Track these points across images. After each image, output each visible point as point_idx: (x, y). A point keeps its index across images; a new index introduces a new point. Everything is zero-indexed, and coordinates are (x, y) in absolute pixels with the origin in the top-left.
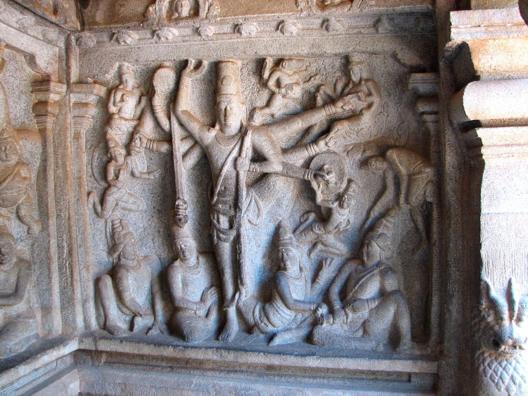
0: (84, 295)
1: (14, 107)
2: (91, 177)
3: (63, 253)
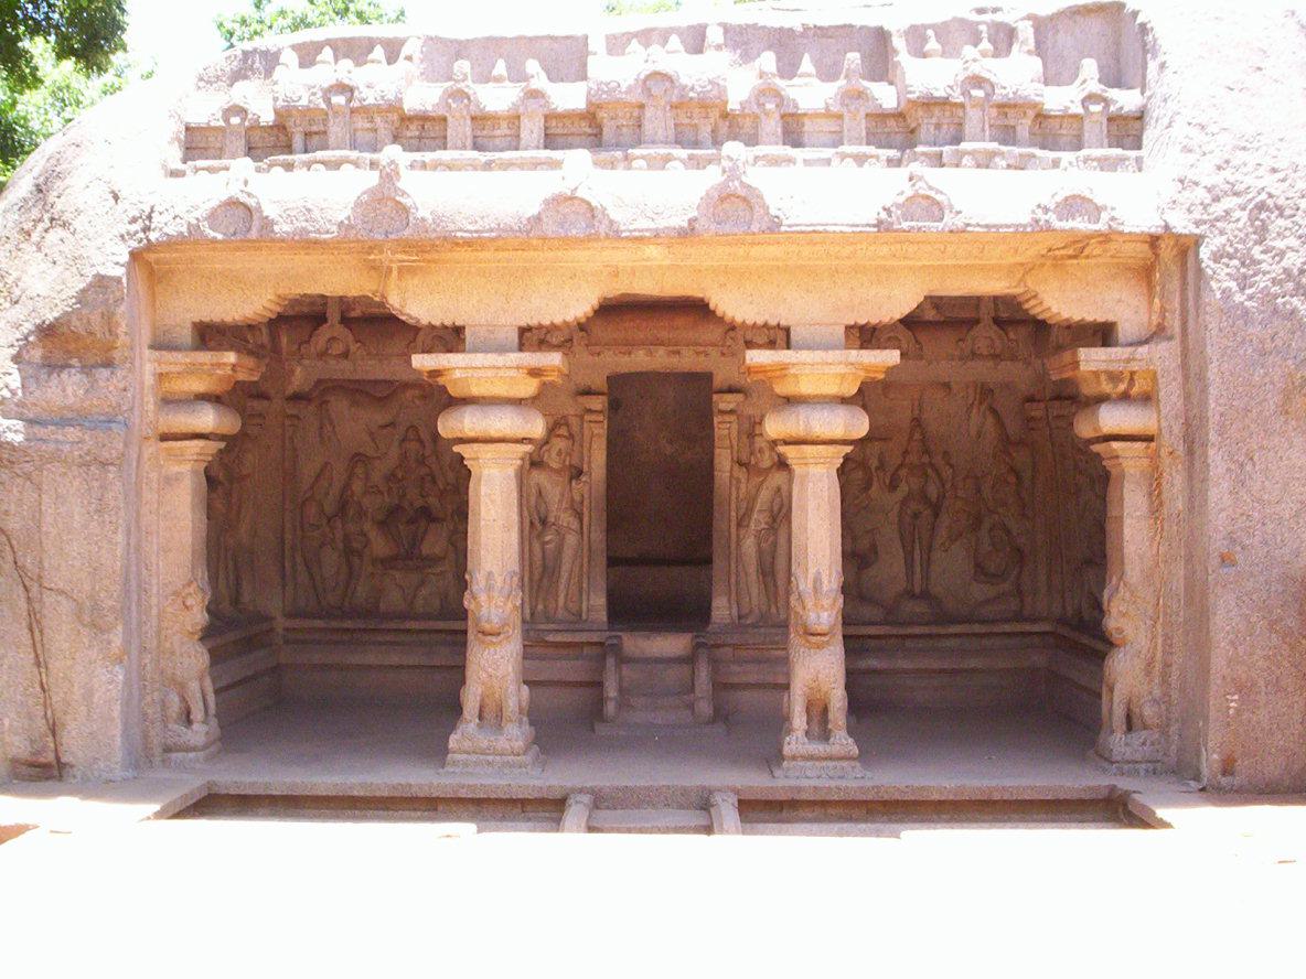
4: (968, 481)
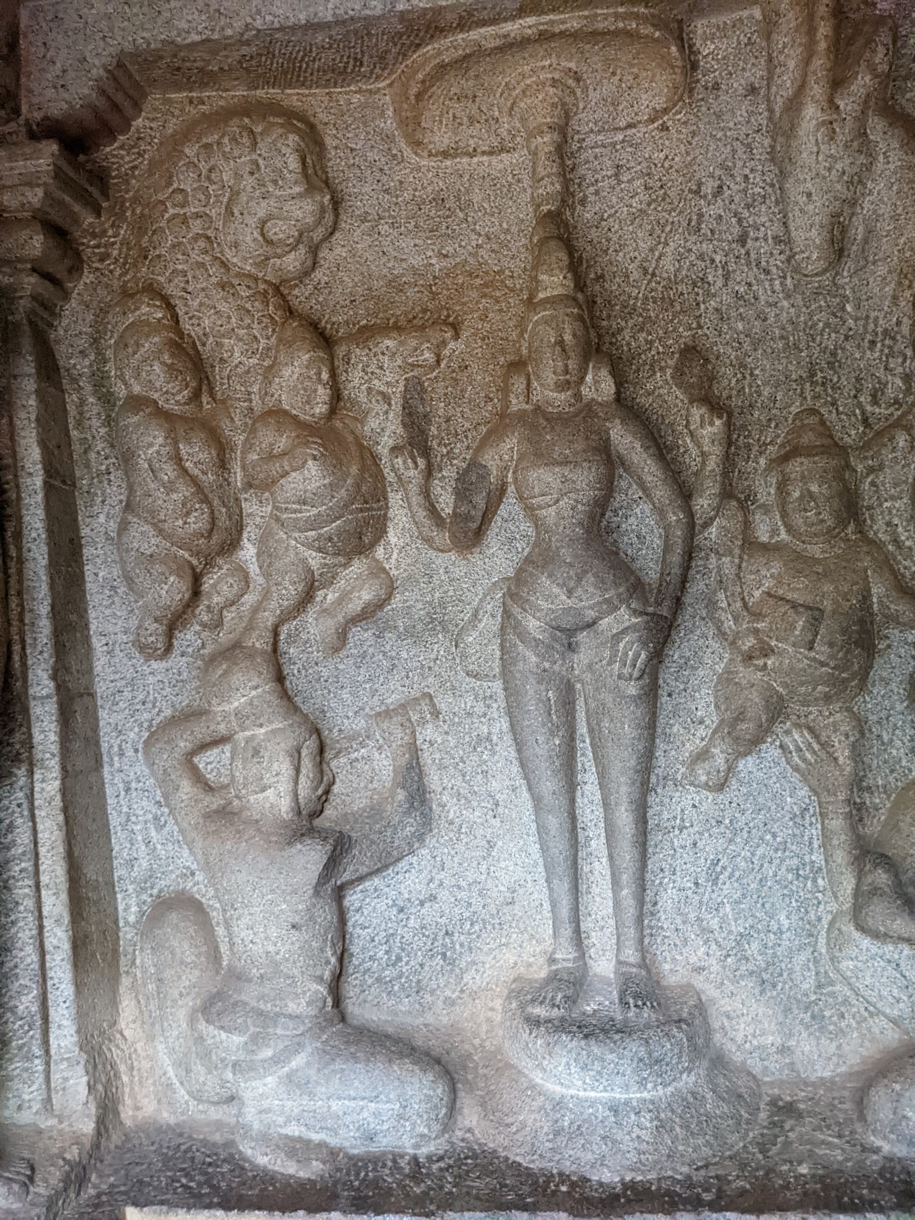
4: (796, 467)
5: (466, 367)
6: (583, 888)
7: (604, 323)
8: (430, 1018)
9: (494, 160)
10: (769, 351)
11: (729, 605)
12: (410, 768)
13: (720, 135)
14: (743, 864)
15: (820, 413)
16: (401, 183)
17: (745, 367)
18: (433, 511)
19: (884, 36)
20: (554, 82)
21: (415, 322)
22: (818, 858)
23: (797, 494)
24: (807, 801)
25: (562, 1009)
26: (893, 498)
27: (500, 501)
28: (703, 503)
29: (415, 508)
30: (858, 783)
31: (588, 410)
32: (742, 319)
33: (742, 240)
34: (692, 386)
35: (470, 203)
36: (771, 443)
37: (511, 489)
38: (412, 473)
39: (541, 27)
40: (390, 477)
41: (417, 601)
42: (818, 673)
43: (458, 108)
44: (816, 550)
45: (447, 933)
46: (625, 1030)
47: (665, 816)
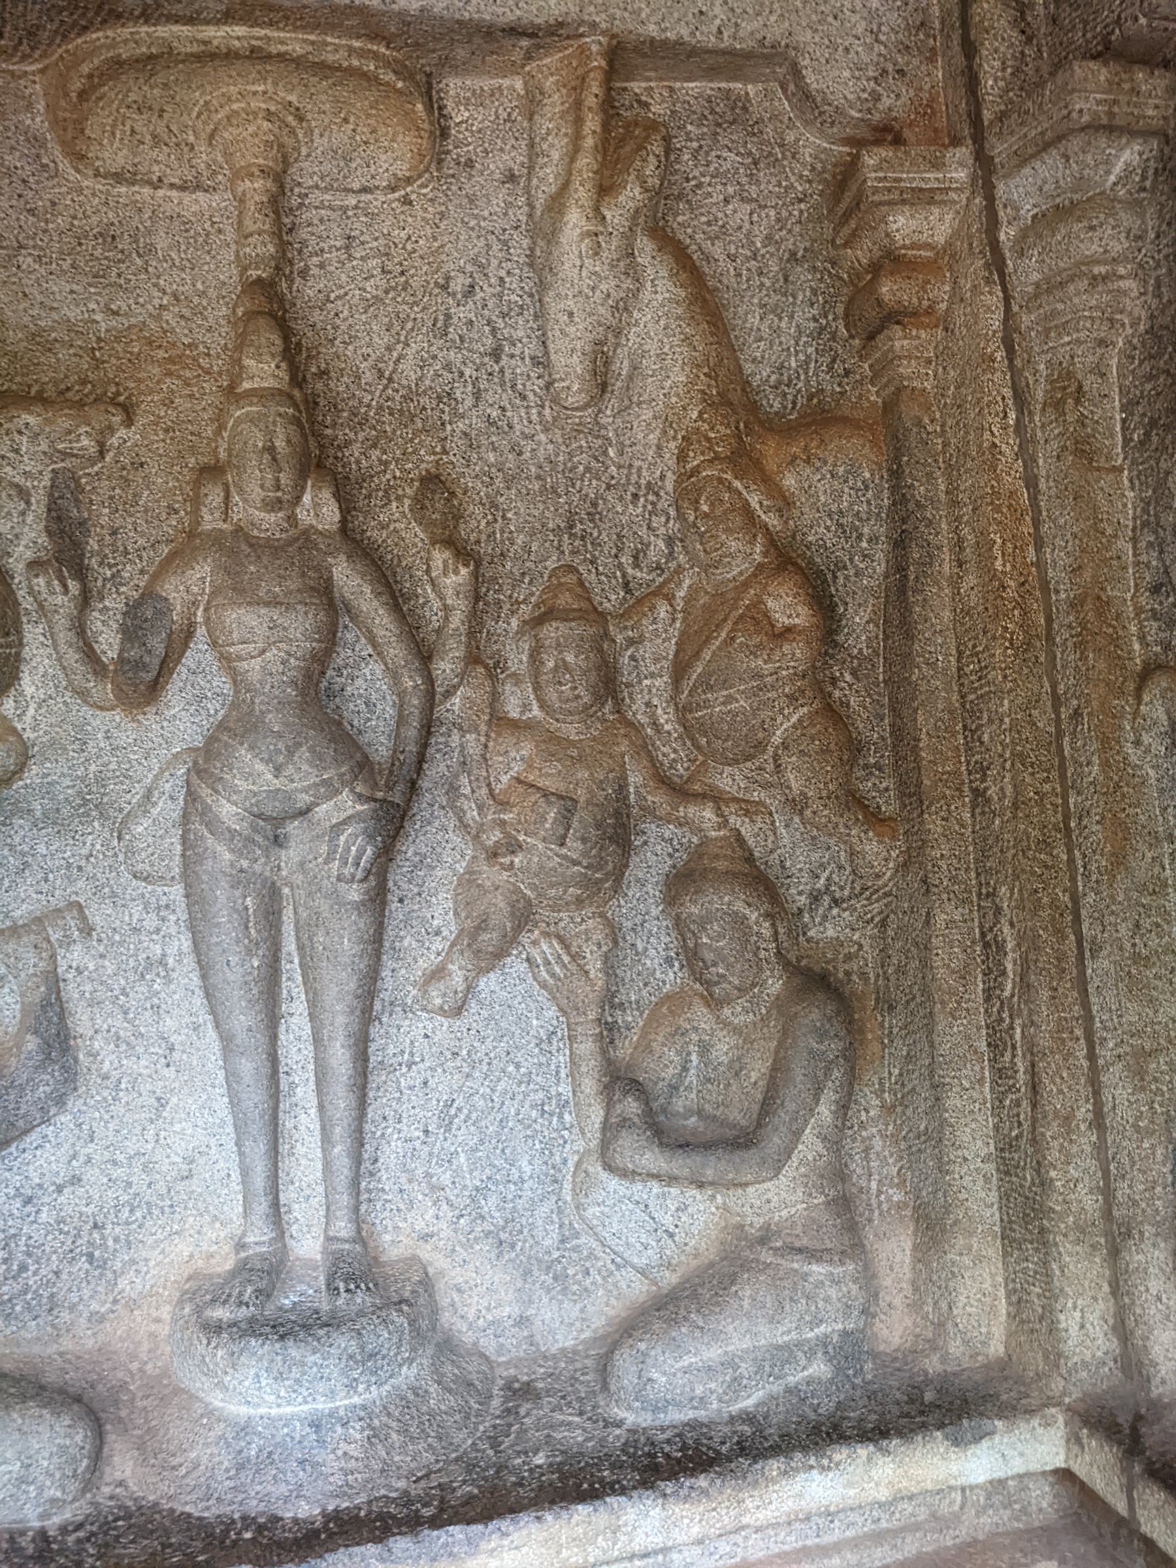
0: (1119, 1194)
1: (766, 331)
2: (1156, 589)
3: (1004, 973)
4: (552, 631)
5: (142, 465)
6: (284, 1148)
7: (328, 432)
8: (67, 1344)
9: (187, 198)
10: (524, 491)
11: (473, 792)
12: (45, 1005)
13: (472, 223)
14: (482, 1103)
15: (577, 571)
16: (54, 204)
17: (496, 507)
18: (90, 654)
19: (657, 148)
20: (269, 115)
21: (69, 395)
22: (565, 1089)
23: (551, 664)
24: (555, 1022)
25: (256, 1308)
26: (652, 675)
27: (186, 646)
28: (445, 667)
29: (63, 648)
30: (610, 1000)
31: (305, 539)
32: (495, 449)
33: (496, 354)
34: (433, 523)
35: (151, 249)
36: (524, 601)
37: (201, 631)
38: (60, 599)
39: (254, 42)
40: (27, 603)
41: (63, 775)
42: (569, 873)
43: (139, 122)
44: (571, 730)
45: (96, 1226)
46: (332, 1322)
47: (391, 1050)
